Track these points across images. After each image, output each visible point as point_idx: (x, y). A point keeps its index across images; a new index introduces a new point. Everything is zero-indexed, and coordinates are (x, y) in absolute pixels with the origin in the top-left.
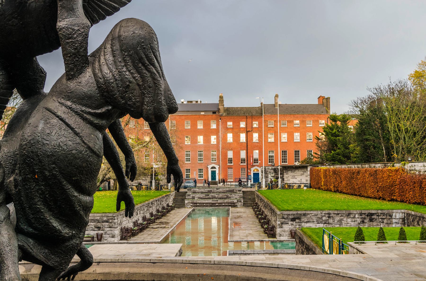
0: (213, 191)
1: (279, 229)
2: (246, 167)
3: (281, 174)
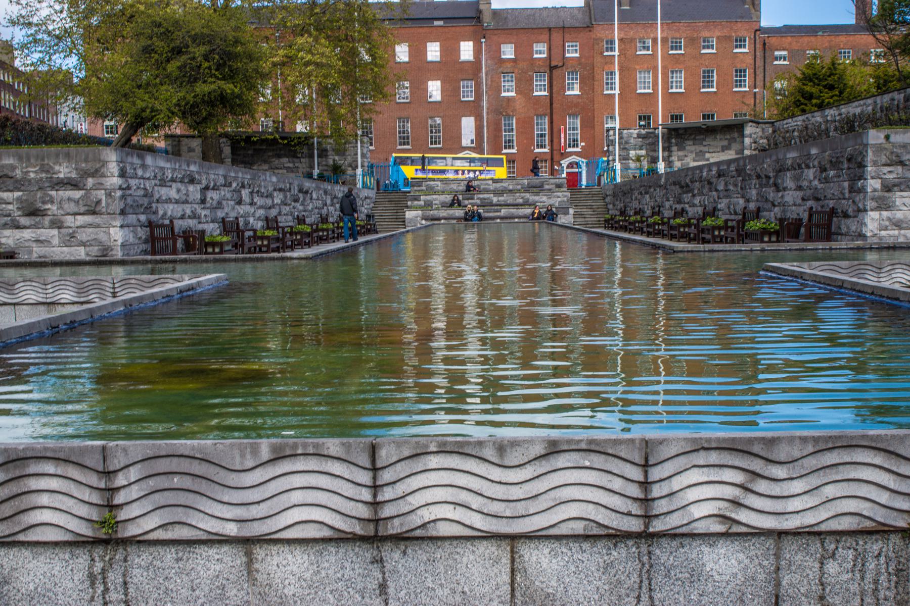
0: (482, 187)
1: (874, 215)
2: (549, 157)
3: (664, 150)
